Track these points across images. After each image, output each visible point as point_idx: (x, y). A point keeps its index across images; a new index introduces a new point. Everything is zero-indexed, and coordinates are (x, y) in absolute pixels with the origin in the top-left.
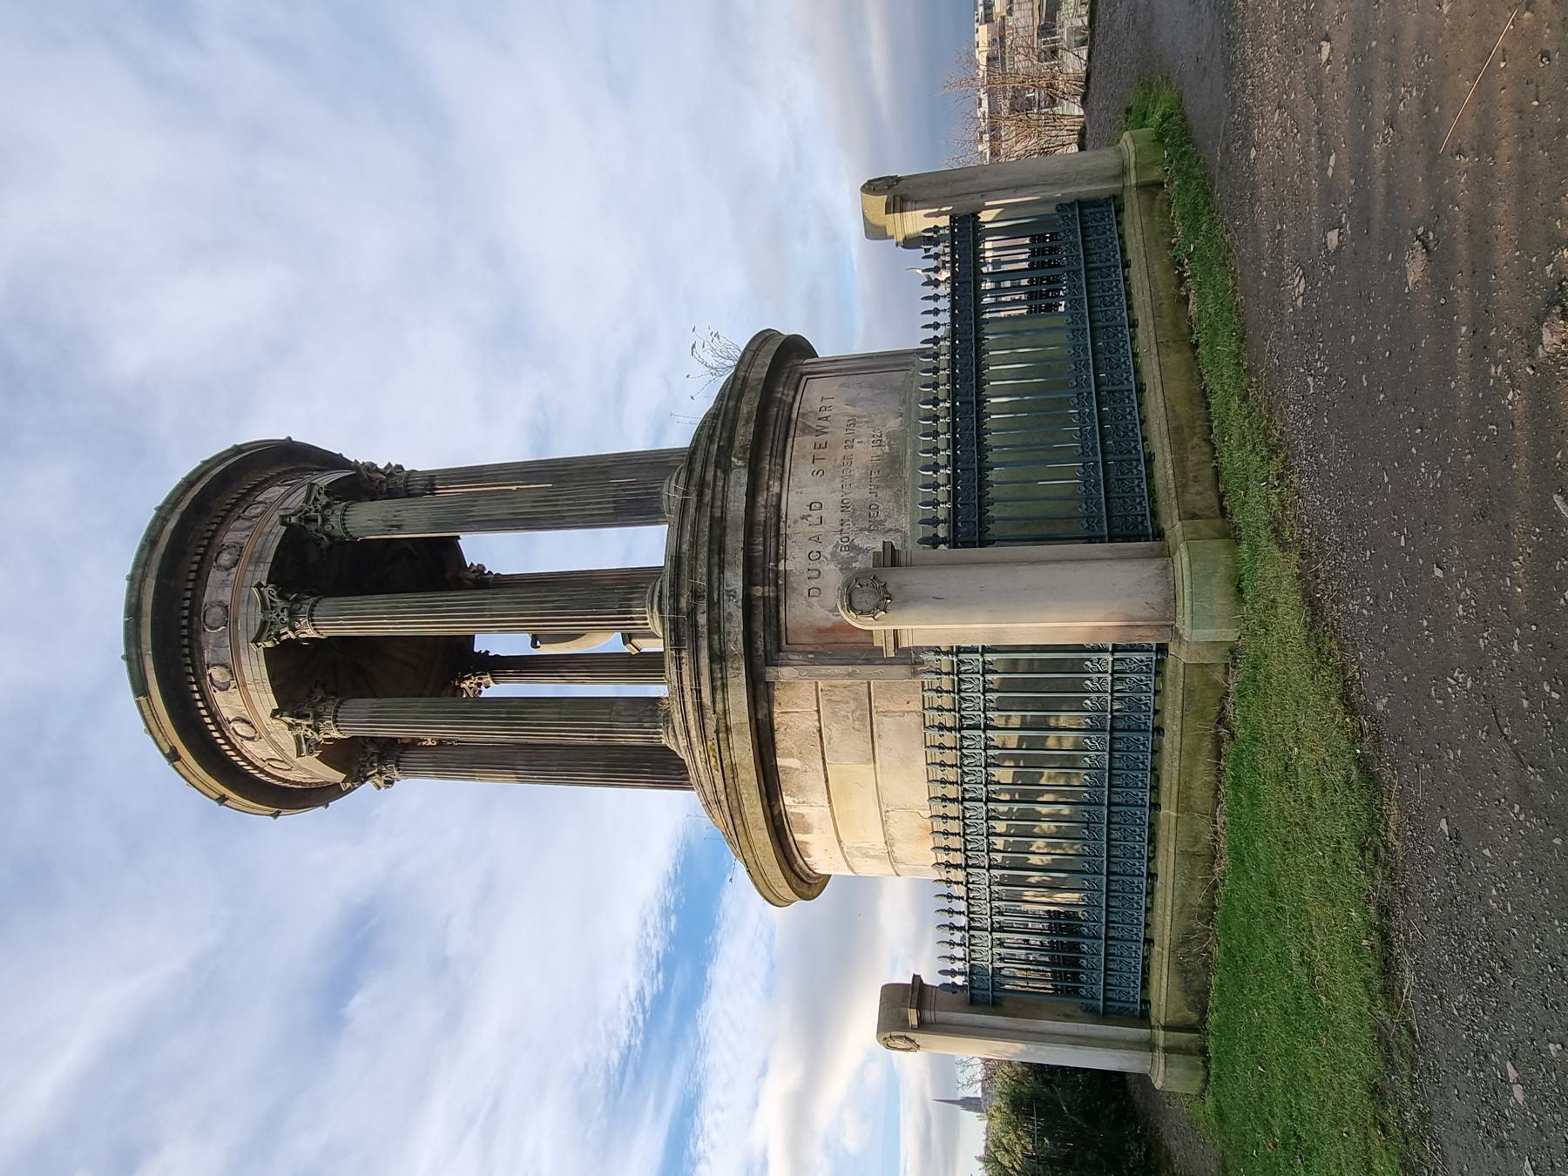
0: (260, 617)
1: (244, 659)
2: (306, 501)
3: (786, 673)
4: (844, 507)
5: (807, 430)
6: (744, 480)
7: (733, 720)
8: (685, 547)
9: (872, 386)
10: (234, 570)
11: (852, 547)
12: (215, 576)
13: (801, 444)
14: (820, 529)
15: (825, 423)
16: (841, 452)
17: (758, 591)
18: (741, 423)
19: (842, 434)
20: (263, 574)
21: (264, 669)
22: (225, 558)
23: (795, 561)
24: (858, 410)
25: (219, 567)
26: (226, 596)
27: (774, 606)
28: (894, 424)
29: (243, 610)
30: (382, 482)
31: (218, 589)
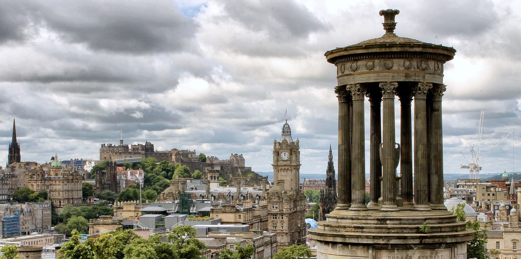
0: (389, 81)
1: (376, 75)
2: (427, 83)
3: (370, 251)
10: (403, 68)
12: (401, 61)
13: (428, 253)
15: (433, 258)
17: (390, 246)
20: (402, 79)
22: (407, 63)
25: (404, 62)
26: (395, 68)
27: (386, 249)
29: (391, 74)
30: (437, 91)
31: (398, 64)
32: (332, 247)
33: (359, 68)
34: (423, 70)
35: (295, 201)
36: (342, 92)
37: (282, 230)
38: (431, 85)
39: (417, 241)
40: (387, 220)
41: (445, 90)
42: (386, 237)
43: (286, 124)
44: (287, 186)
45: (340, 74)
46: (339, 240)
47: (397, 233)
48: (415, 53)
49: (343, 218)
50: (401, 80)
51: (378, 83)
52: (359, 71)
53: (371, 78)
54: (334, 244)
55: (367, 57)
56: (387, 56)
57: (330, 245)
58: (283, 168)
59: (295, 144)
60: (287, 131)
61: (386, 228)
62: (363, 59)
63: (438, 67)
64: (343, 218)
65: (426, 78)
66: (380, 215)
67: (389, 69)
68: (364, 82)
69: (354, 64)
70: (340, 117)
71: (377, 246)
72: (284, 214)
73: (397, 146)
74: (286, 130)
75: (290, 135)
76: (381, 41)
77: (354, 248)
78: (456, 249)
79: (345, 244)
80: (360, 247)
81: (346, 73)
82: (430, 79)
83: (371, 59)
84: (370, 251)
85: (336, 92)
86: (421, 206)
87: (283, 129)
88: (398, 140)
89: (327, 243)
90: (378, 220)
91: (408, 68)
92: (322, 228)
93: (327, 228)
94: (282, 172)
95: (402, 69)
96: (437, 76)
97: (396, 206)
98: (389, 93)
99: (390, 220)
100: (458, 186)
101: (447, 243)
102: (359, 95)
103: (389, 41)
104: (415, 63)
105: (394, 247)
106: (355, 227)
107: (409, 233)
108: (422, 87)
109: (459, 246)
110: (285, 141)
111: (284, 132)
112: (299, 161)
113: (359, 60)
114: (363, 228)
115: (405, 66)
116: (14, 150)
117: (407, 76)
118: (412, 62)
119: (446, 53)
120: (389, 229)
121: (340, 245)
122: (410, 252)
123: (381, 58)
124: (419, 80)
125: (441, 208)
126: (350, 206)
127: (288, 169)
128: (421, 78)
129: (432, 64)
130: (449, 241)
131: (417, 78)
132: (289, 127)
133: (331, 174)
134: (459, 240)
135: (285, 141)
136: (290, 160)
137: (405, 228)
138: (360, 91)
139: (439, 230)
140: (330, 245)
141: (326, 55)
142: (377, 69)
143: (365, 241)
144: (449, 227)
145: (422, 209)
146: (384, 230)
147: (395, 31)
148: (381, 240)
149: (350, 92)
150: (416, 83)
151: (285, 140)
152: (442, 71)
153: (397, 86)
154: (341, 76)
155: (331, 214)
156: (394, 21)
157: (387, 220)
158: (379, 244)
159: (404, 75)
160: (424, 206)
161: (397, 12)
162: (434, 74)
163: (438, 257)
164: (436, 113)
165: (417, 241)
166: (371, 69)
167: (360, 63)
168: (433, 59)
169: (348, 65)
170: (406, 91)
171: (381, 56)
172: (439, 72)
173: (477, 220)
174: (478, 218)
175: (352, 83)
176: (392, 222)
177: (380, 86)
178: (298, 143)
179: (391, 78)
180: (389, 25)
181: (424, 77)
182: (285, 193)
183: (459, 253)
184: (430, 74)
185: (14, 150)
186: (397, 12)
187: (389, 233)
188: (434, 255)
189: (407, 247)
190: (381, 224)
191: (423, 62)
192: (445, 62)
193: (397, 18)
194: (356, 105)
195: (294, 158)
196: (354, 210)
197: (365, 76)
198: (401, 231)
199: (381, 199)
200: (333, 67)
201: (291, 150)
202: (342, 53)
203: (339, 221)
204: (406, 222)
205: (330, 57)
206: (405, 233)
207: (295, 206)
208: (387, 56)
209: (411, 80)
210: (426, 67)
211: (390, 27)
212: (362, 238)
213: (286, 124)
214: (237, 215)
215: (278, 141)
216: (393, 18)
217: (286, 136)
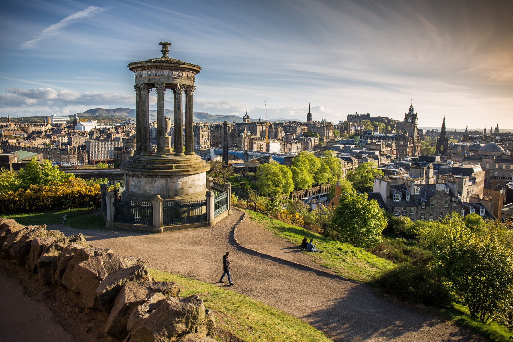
5: (152, 181)
9: (161, 189)
12: (147, 71)
13: (150, 180)
22: (150, 73)
23: (135, 179)
26: (144, 76)
28: (152, 193)
31: (145, 73)
39: (140, 173)
48: (148, 66)
60: (411, 109)
91: (150, 75)
95: (147, 76)
99: (138, 160)
104: (154, 72)
108: (158, 86)
109: (175, 178)
110: (410, 113)
116: (309, 116)
117: (149, 80)
130: (159, 174)
134: (169, 174)
147: (168, 55)
168: (167, 69)
185: (309, 116)
207: (413, 143)
209: (152, 82)
211: (165, 53)
214: (377, 146)
215: (407, 113)
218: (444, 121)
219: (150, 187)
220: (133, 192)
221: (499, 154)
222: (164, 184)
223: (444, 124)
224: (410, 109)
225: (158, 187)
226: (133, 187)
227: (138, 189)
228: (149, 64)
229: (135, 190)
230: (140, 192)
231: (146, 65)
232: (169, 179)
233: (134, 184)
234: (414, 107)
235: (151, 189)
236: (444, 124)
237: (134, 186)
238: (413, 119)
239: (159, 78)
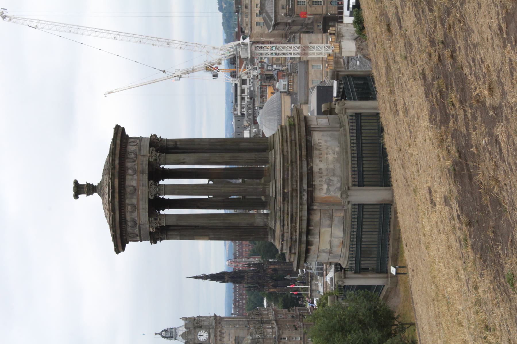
1: (141, 203)
4: (327, 169)
5: (316, 149)
6: (306, 163)
7: (303, 218)
8: (285, 176)
11: (330, 180)
12: (128, 178)
13: (316, 153)
14: (321, 175)
16: (326, 156)
17: (309, 189)
18: (303, 149)
19: (325, 151)
20: (146, 177)
21: (147, 206)
22: (130, 172)
24: (328, 144)
25: (129, 175)
26: (134, 183)
28: (337, 149)
29: (141, 188)
30: (157, 143)
31: (131, 181)
32: (312, 245)
33: (133, 219)
34: (136, 157)
35: (262, 322)
36: (156, 237)
37: (301, 339)
38: (151, 148)
40: (284, 192)
41: (155, 136)
42: (301, 192)
43: (161, 334)
44: (242, 333)
45: (138, 238)
46: (304, 238)
47: (296, 181)
49: (283, 236)
50: (147, 177)
51: (150, 201)
52: (137, 219)
53: (144, 206)
54: (309, 244)
55: (123, 211)
56: (123, 191)
57: (310, 247)
58: (219, 338)
59: (187, 322)
61: (292, 194)
62: (125, 215)
63: (134, 142)
64: (283, 236)
65: (145, 154)
66: (279, 198)
67: (135, 190)
68: (147, 214)
69: (130, 224)
70: (181, 238)
71: (309, 201)
72: (279, 336)
73: (211, 182)
74: (169, 334)
75: (175, 329)
76: (107, 197)
77: (313, 224)
78: (312, 126)
79: (309, 232)
80: (311, 217)
81: (137, 233)
82: (146, 149)
83: (125, 207)
84: (315, 208)
85: (155, 243)
86: (270, 159)
87: (167, 338)
88: (205, 181)
89: (308, 251)
90: (284, 200)
91: (135, 171)
92: (293, 256)
93: (293, 251)
94: (225, 339)
95: (135, 177)
96: (142, 144)
97: (271, 183)
98: (159, 190)
99: (284, 189)
100: (243, 114)
101: (306, 135)
102: (160, 219)
103: (107, 190)
105: (311, 184)
106: (292, 223)
107: (296, 171)
108: (154, 158)
109: (310, 123)
110: (184, 336)
111: (172, 337)
112: (210, 317)
113: (125, 219)
114: (292, 215)
115: (132, 173)
117: (142, 172)
118: (129, 167)
119: (119, 135)
120: (292, 189)
121: (309, 237)
122: (316, 169)
123: (125, 197)
124: (146, 160)
125: (272, 140)
126: (271, 228)
127: (220, 331)
128: (145, 159)
129: (131, 148)
130: (304, 133)
131: (145, 163)
132: (165, 330)
133: (226, 277)
135: (184, 336)
136: (208, 329)
137: (292, 174)
138: (156, 218)
139: (293, 142)
140: (310, 247)
141: (117, 251)
142: (134, 201)
143: (305, 213)
144: (290, 131)
145: (273, 158)
146: (294, 194)
147: (95, 184)
148: (303, 197)
149: (156, 228)
150: (150, 164)
151: (182, 336)
152: (137, 138)
153: (152, 181)
154: (140, 237)
155: (278, 245)
156: (83, 185)
157: (284, 192)
158: (308, 199)
159: (142, 175)
160: (270, 157)
161: (76, 182)
162: (140, 146)
163: (320, 143)
164: (178, 144)
165: (305, 163)
166: (135, 207)
167: (128, 218)
169: (129, 230)
170: (156, 174)
171: (123, 197)
172: (138, 141)
173: (286, 92)
174: (282, 90)
175: (148, 226)
176: (286, 187)
177: (152, 198)
178: (185, 319)
179: (144, 188)
180: (89, 189)
181: (143, 156)
182: (251, 334)
183: (316, 123)
184: (140, 150)
186: (76, 182)
187: (297, 190)
188: (318, 147)
189: (310, 173)
190: (288, 197)
191: (129, 156)
192: (128, 135)
193: (82, 182)
194: (170, 222)
195: (206, 323)
196: (275, 224)
197: (141, 213)
198: (295, 178)
199: (263, 198)
200: (130, 246)
201: (195, 328)
202: (118, 236)
203: (285, 238)
204: (286, 173)
205: (120, 249)
206: (297, 175)
207: (269, 322)
208: (123, 191)
209: (146, 168)
210: (134, 154)
211: (90, 189)
212: (302, 216)
213: (161, 334)
216: (82, 186)
217: (176, 335)
218: (204, 277)
219: (327, 154)
220: (340, 189)
221: (287, 99)
222: (321, 133)
223: (214, 277)
224: (171, 337)
225: (326, 141)
226: (332, 189)
227: (334, 175)
228: (117, 162)
229: (337, 183)
230: (338, 171)
231: (117, 167)
232: (312, 126)
233: (325, 187)
234: (166, 328)
235: (330, 151)
236: (214, 277)
237: (328, 185)
238: (201, 327)
239: (141, 158)
